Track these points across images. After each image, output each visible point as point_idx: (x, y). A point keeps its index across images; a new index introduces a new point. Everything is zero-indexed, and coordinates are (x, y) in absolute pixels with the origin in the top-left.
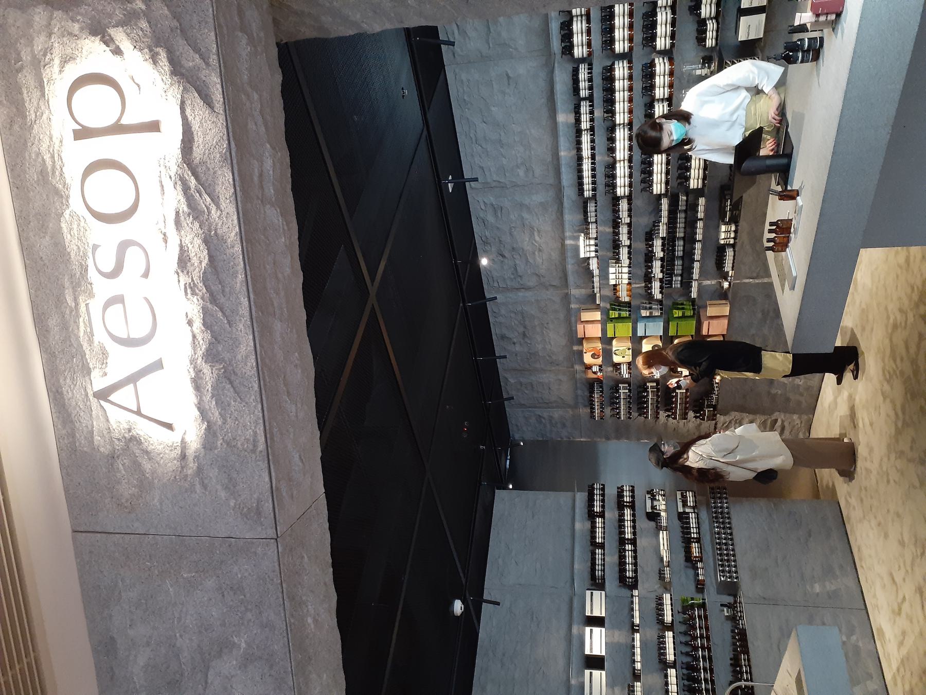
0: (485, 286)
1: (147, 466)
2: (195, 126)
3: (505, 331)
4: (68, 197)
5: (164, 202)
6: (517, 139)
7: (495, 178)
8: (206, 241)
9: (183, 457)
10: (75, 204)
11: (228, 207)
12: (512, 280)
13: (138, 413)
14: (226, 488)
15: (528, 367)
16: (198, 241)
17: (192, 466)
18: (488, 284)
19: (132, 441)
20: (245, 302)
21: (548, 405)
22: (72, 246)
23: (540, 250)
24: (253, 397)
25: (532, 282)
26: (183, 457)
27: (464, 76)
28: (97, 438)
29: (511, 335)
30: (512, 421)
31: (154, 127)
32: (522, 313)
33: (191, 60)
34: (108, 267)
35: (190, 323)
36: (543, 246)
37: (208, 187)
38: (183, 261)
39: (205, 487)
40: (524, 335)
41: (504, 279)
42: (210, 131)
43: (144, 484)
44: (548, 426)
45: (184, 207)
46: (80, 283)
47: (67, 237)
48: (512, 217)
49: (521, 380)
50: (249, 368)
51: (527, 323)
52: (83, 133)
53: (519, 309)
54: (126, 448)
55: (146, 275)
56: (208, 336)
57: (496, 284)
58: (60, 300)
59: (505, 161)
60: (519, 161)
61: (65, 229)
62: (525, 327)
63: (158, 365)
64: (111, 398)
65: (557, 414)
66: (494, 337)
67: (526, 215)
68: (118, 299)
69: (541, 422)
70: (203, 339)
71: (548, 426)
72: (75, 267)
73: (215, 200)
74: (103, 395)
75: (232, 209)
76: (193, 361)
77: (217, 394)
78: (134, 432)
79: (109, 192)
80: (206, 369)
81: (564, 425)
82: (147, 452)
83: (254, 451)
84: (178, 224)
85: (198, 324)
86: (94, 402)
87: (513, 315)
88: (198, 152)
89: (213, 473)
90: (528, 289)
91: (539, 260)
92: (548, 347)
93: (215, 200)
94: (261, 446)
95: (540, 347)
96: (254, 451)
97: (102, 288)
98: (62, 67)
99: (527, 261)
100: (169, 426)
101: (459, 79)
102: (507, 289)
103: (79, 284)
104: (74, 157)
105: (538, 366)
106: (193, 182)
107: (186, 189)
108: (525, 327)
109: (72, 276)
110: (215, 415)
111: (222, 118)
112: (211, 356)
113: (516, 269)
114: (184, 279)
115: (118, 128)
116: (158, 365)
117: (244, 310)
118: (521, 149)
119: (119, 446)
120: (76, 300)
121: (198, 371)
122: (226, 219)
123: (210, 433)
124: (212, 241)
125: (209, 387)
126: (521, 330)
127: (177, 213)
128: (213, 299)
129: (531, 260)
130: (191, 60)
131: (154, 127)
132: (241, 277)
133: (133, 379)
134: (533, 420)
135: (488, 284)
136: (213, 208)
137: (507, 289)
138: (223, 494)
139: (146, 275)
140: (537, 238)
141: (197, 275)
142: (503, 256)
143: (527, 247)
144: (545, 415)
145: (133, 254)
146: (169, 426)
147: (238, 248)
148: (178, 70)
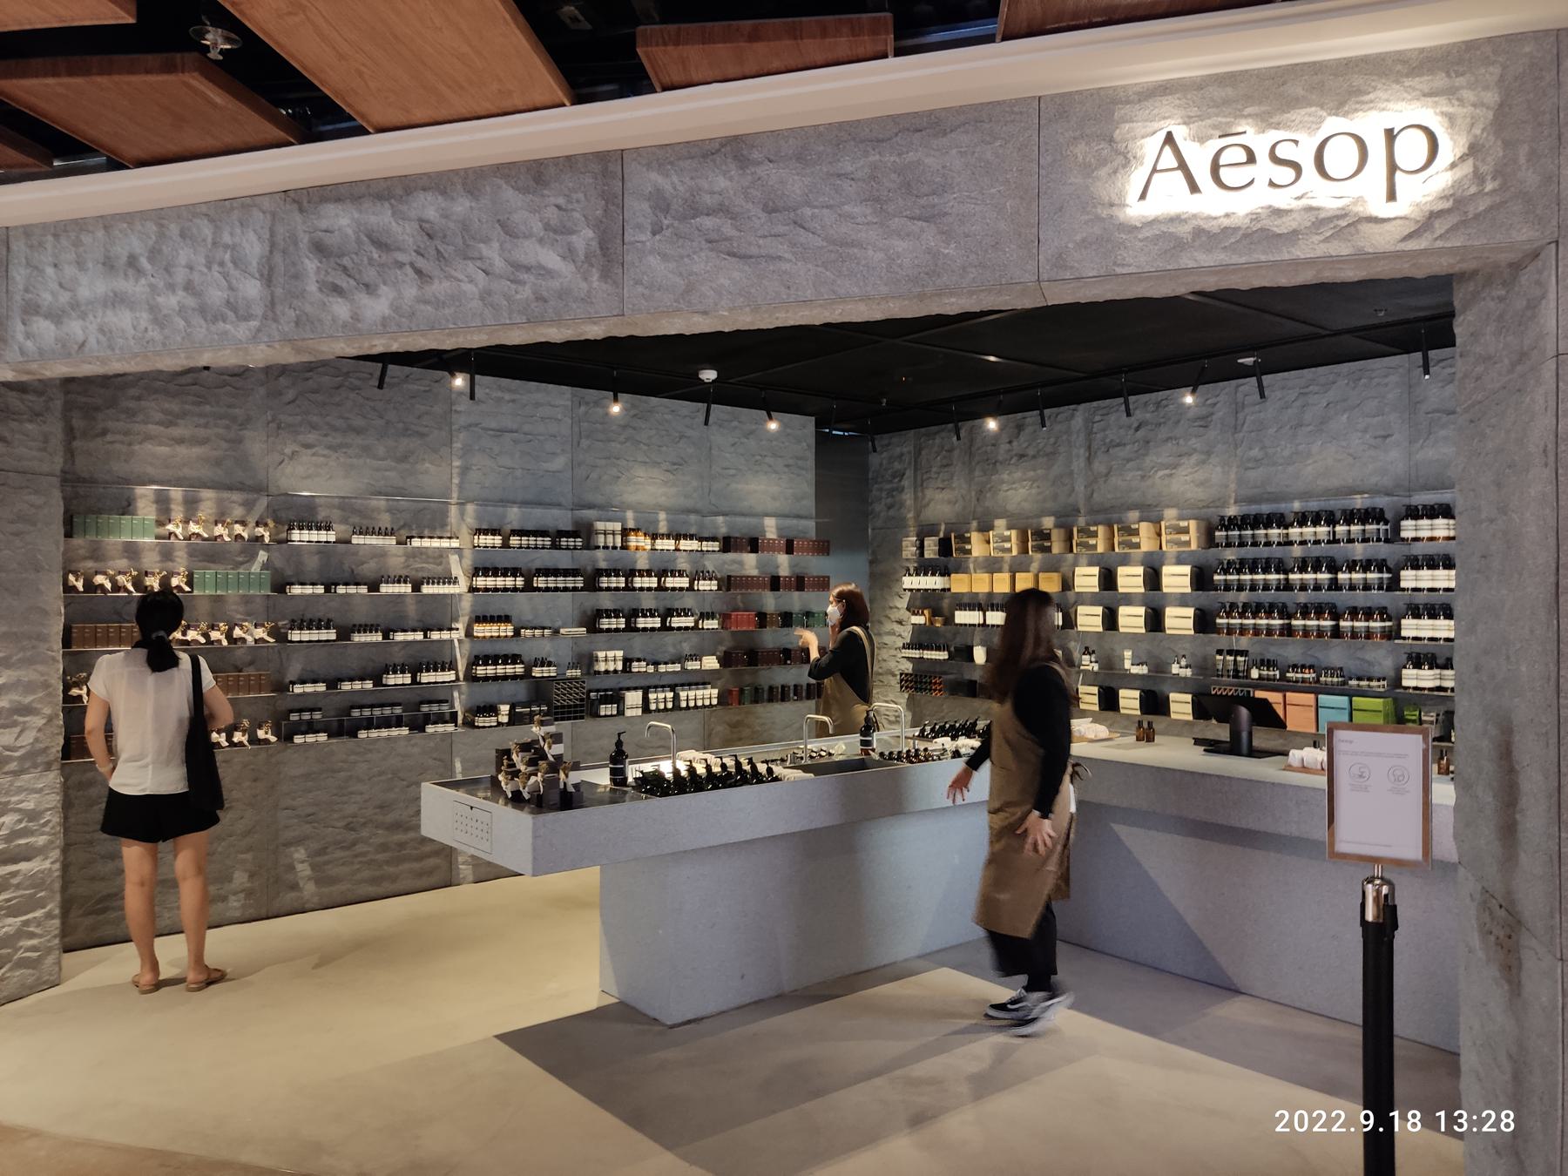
0: (1095, 404)
1: (1103, 172)
2: (1387, 226)
3: (1029, 430)
4: (1337, 115)
5: (1325, 196)
6: (1301, 448)
7: (1250, 418)
8: (1295, 232)
9: (1112, 205)
10: (1333, 124)
11: (1321, 250)
12: (1103, 440)
13: (1154, 170)
14: (1084, 240)
15: (977, 458)
16: (1294, 225)
17: (1104, 213)
18: (1098, 408)
19: (1126, 160)
20: (1243, 260)
21: (919, 486)
22: (1297, 115)
23: (1143, 477)
24: (1161, 264)
25: (1099, 466)
26: (1112, 205)
27: (1393, 379)
28: (1127, 126)
29: (1022, 438)
30: (896, 438)
31: (1392, 196)
32: (1053, 453)
33: (1440, 227)
34: (1280, 153)
35: (1227, 215)
36: (1149, 482)
37: (1339, 234)
38: (1277, 213)
39: (1086, 223)
40: (1022, 456)
41: (1104, 430)
42: (1381, 240)
43: (1088, 169)
44: (888, 486)
45: (1323, 215)
46: (1266, 121)
47: (1303, 112)
48: (1193, 440)
49: (956, 453)
50: (1186, 261)
51: (1040, 460)
52: (1390, 135)
53: (1062, 449)
54: (1118, 153)
55: (1272, 184)
56: (1216, 230)
57: (1097, 418)
58: (1249, 99)
59: (1271, 431)
60: (1270, 451)
61: (1309, 110)
62: (1034, 457)
63: (1194, 188)
64: (1167, 149)
65: (908, 498)
66: (1020, 415)
67: (1194, 458)
68: (1251, 159)
69: (894, 477)
70: (1212, 226)
71: (888, 486)
72: (1276, 119)
73: (1326, 240)
74: (1169, 139)
75: (1319, 253)
76: (1195, 216)
77: (1163, 236)
78: (1133, 162)
79: (1341, 157)
80: (1188, 228)
81: (889, 507)
82: (1115, 172)
83: (1115, 264)
84: (1310, 209)
85: (1226, 222)
86: (1162, 136)
87: (1052, 440)
88: (1365, 228)
89: (1097, 230)
90: (1089, 460)
91: (1129, 476)
92: (1005, 487)
93: (1326, 240)
94: (1119, 270)
95: (1005, 477)
96: (1115, 264)
97: (1261, 142)
98: (1443, 114)
99: (1129, 460)
100: (1143, 196)
101: (1393, 370)
102: (1090, 434)
103: (1263, 120)
104: (1370, 123)
105: (977, 473)
106: (1343, 223)
107: (1338, 217)
108: (1034, 457)
109: (1270, 114)
110: (1147, 233)
111: (1392, 249)
112: (1198, 232)
113: (1118, 445)
114: (1264, 213)
115: (1392, 168)
116: (1194, 188)
117: (1236, 259)
118: (1286, 453)
119: (1121, 147)
120: (1249, 116)
121: (1185, 221)
122: (1313, 248)
123: (1131, 229)
124: (1294, 234)
125: (1172, 230)
126: (1031, 452)
127: (1318, 209)
128: (1246, 236)
129: (1129, 466)
130: (1440, 227)
131: (1392, 196)
132: (1263, 258)
133: (1183, 166)
134: (897, 466)
135: (1098, 408)
136: (1321, 238)
137: (1090, 434)
138: (1078, 238)
139: (1272, 184)
140: (1161, 473)
141: (1266, 223)
142: (1137, 429)
143: (1149, 461)
144: (905, 483)
145: (1289, 173)
146: (1143, 196)
147: (1286, 257)
148: (1433, 216)
